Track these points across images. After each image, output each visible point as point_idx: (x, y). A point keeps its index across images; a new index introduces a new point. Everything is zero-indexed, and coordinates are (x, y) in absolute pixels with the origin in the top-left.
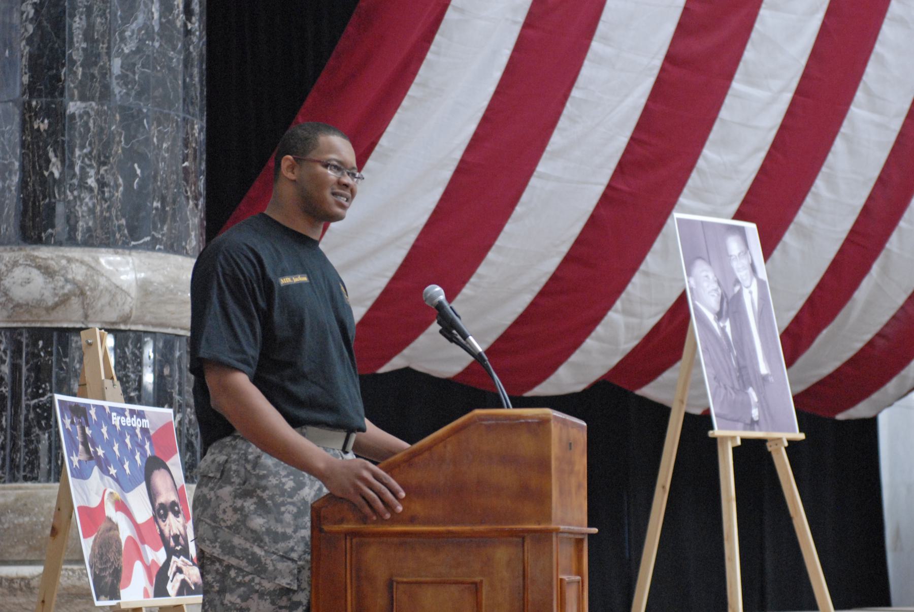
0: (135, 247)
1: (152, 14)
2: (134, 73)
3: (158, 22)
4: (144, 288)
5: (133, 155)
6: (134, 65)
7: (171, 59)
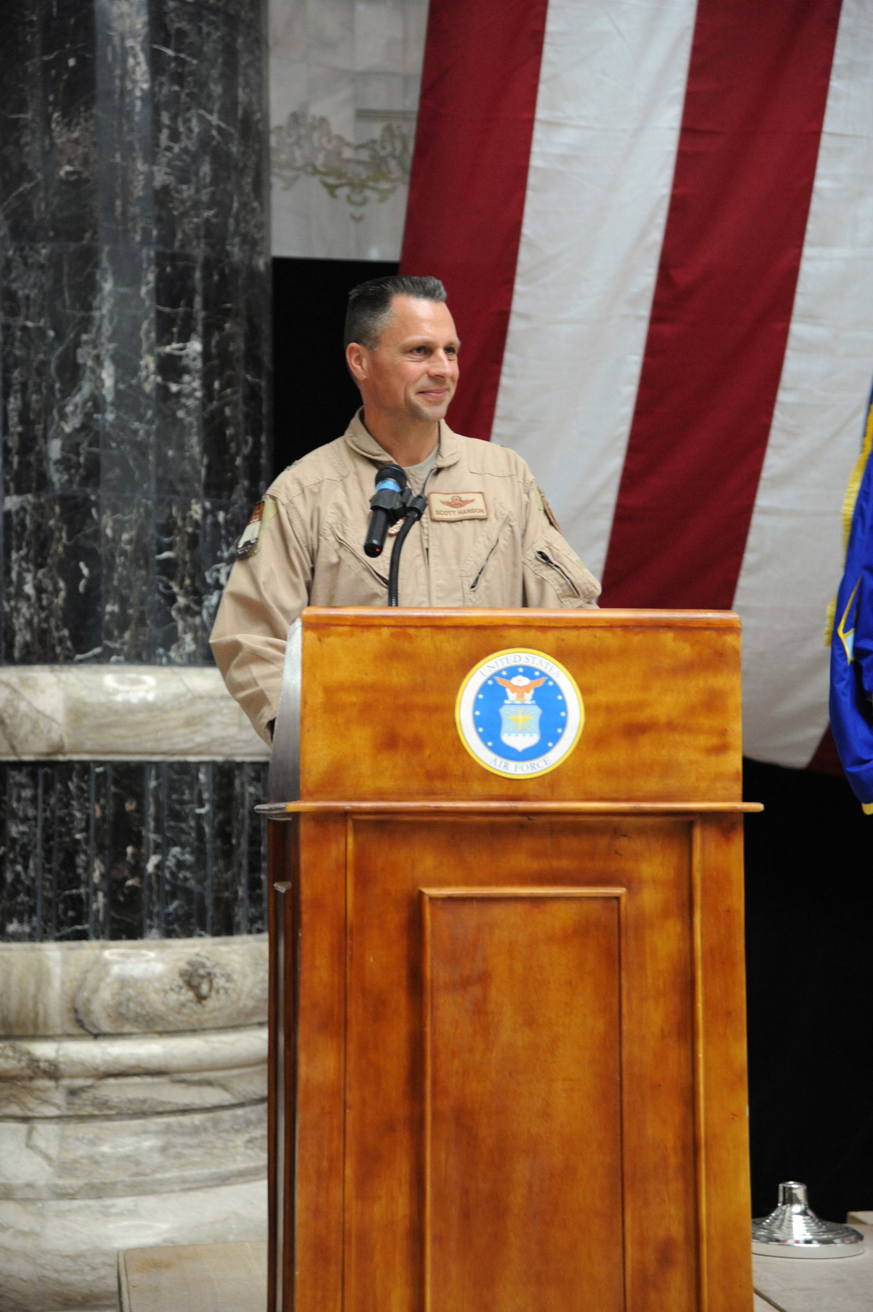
0: (81, 661)
1: (102, 380)
2: (78, 454)
3: (112, 390)
4: (78, 713)
5: (75, 553)
6: (78, 445)
7: (136, 432)
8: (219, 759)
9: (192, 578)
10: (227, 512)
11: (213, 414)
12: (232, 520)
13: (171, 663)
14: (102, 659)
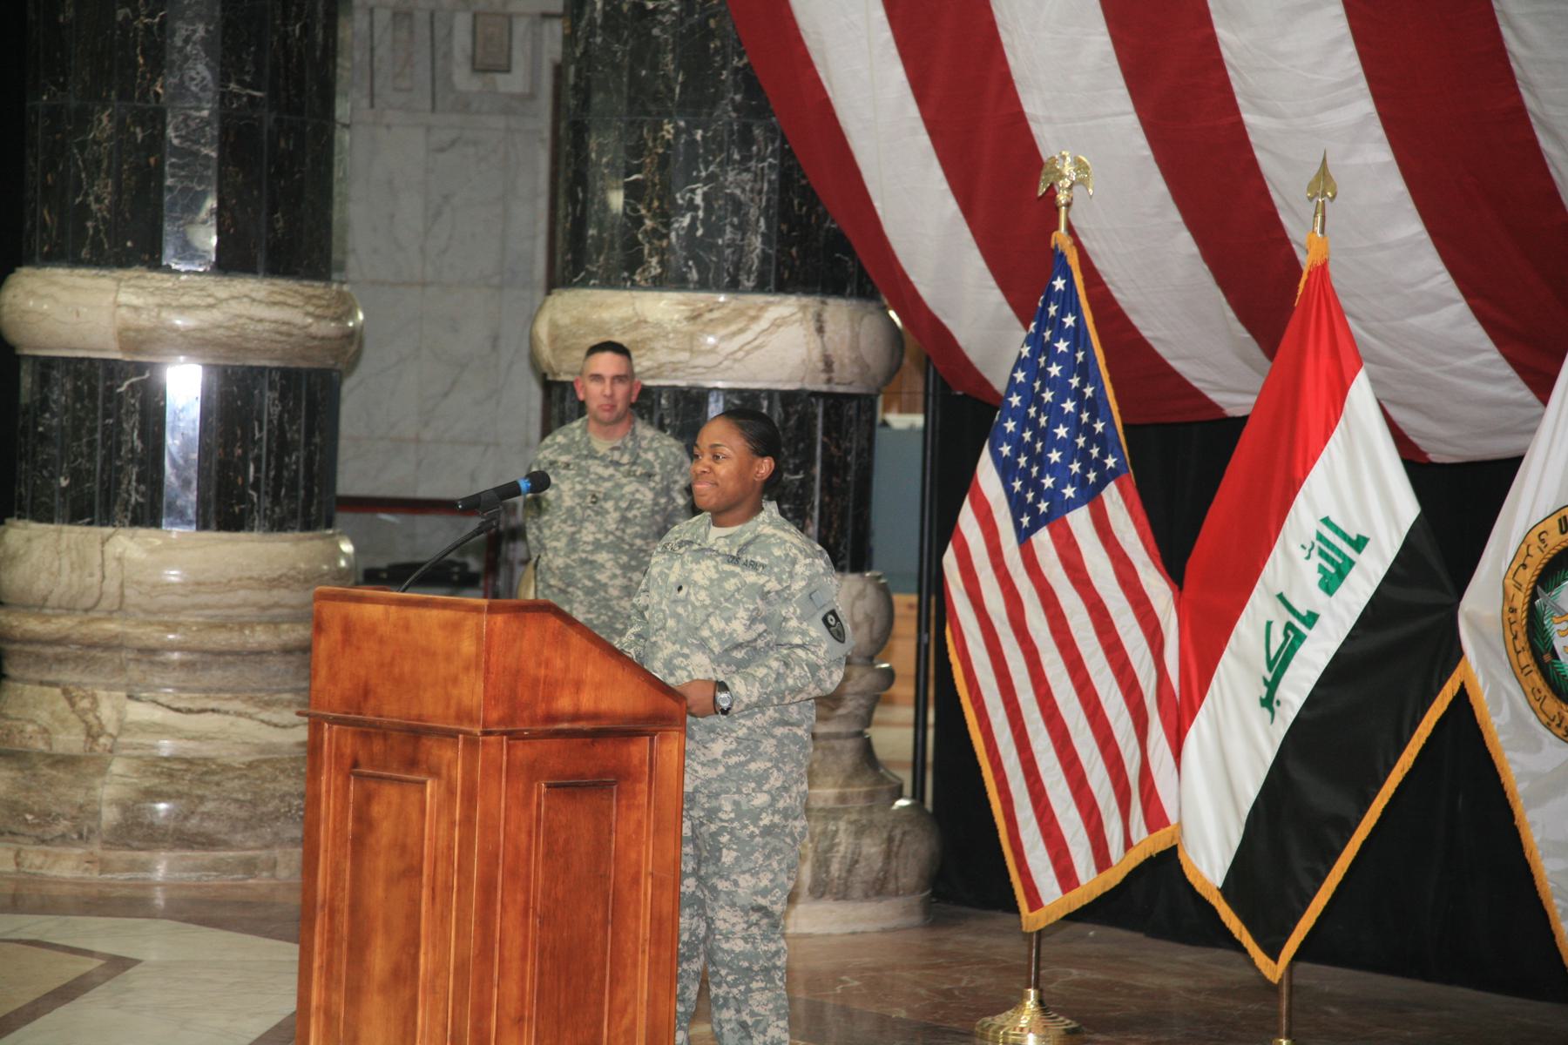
8: (682, 383)
9: (660, 199)
10: (705, 131)
11: (692, 29)
12: (714, 138)
13: (635, 286)
14: (584, 284)
